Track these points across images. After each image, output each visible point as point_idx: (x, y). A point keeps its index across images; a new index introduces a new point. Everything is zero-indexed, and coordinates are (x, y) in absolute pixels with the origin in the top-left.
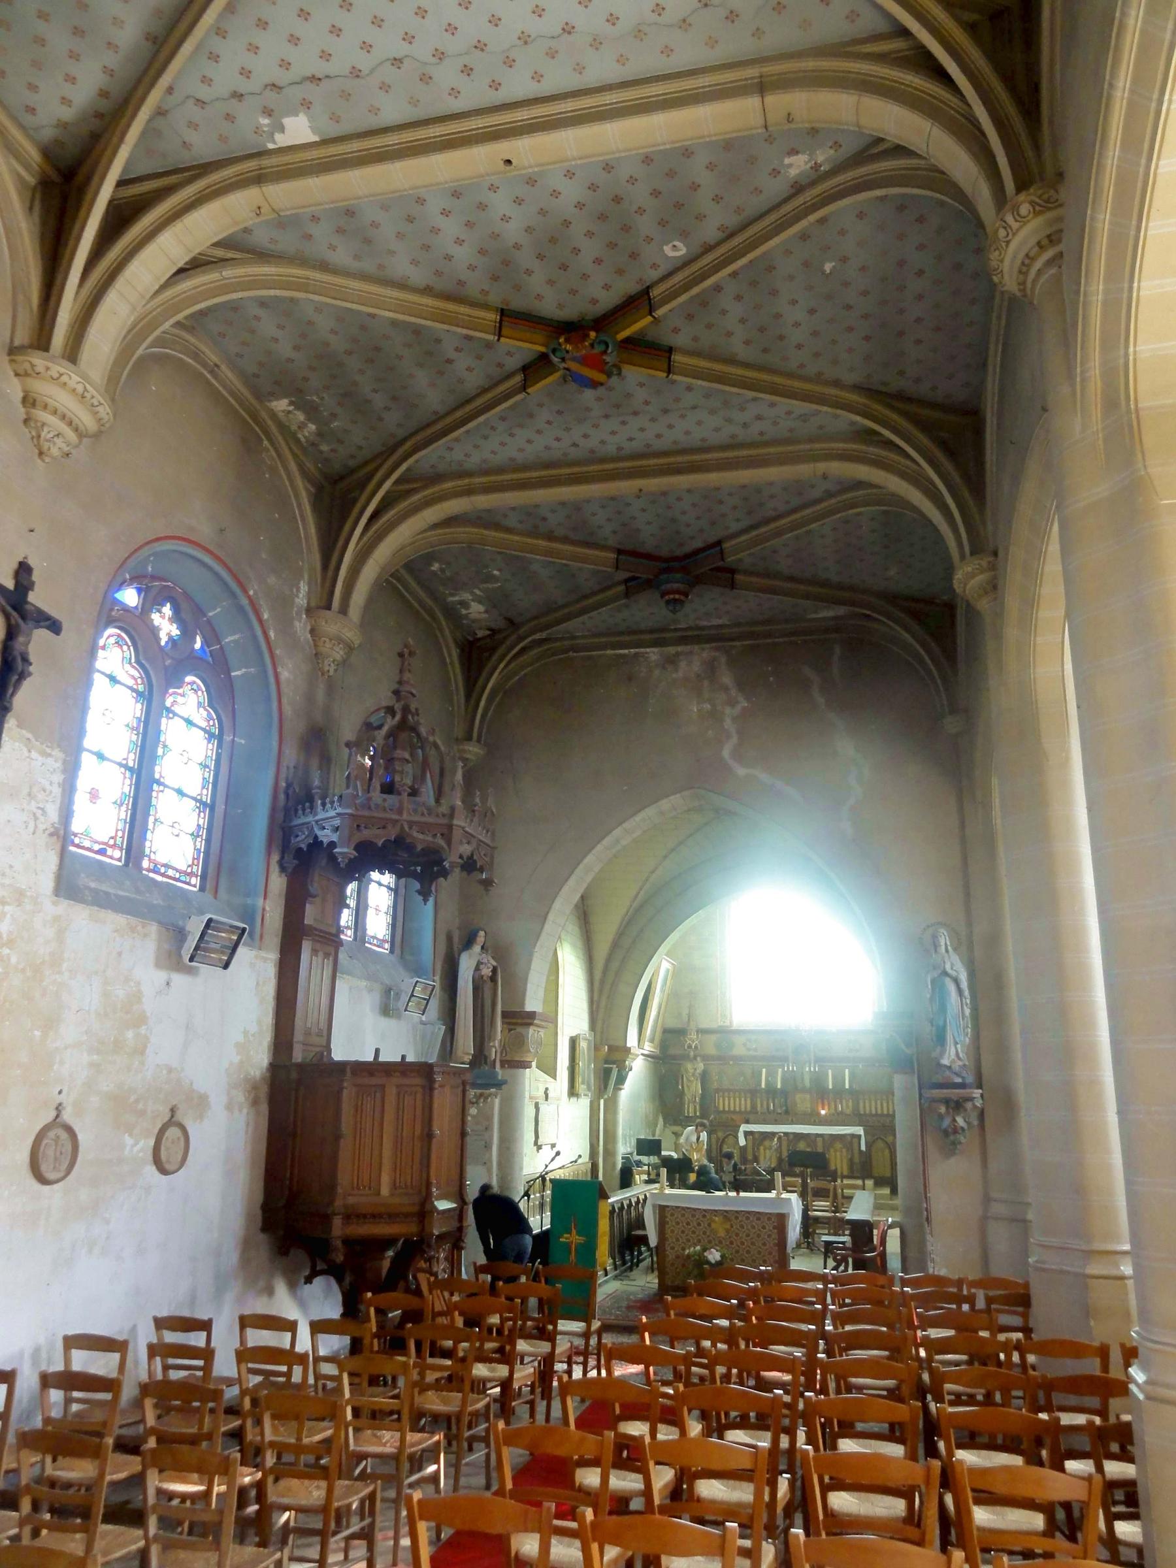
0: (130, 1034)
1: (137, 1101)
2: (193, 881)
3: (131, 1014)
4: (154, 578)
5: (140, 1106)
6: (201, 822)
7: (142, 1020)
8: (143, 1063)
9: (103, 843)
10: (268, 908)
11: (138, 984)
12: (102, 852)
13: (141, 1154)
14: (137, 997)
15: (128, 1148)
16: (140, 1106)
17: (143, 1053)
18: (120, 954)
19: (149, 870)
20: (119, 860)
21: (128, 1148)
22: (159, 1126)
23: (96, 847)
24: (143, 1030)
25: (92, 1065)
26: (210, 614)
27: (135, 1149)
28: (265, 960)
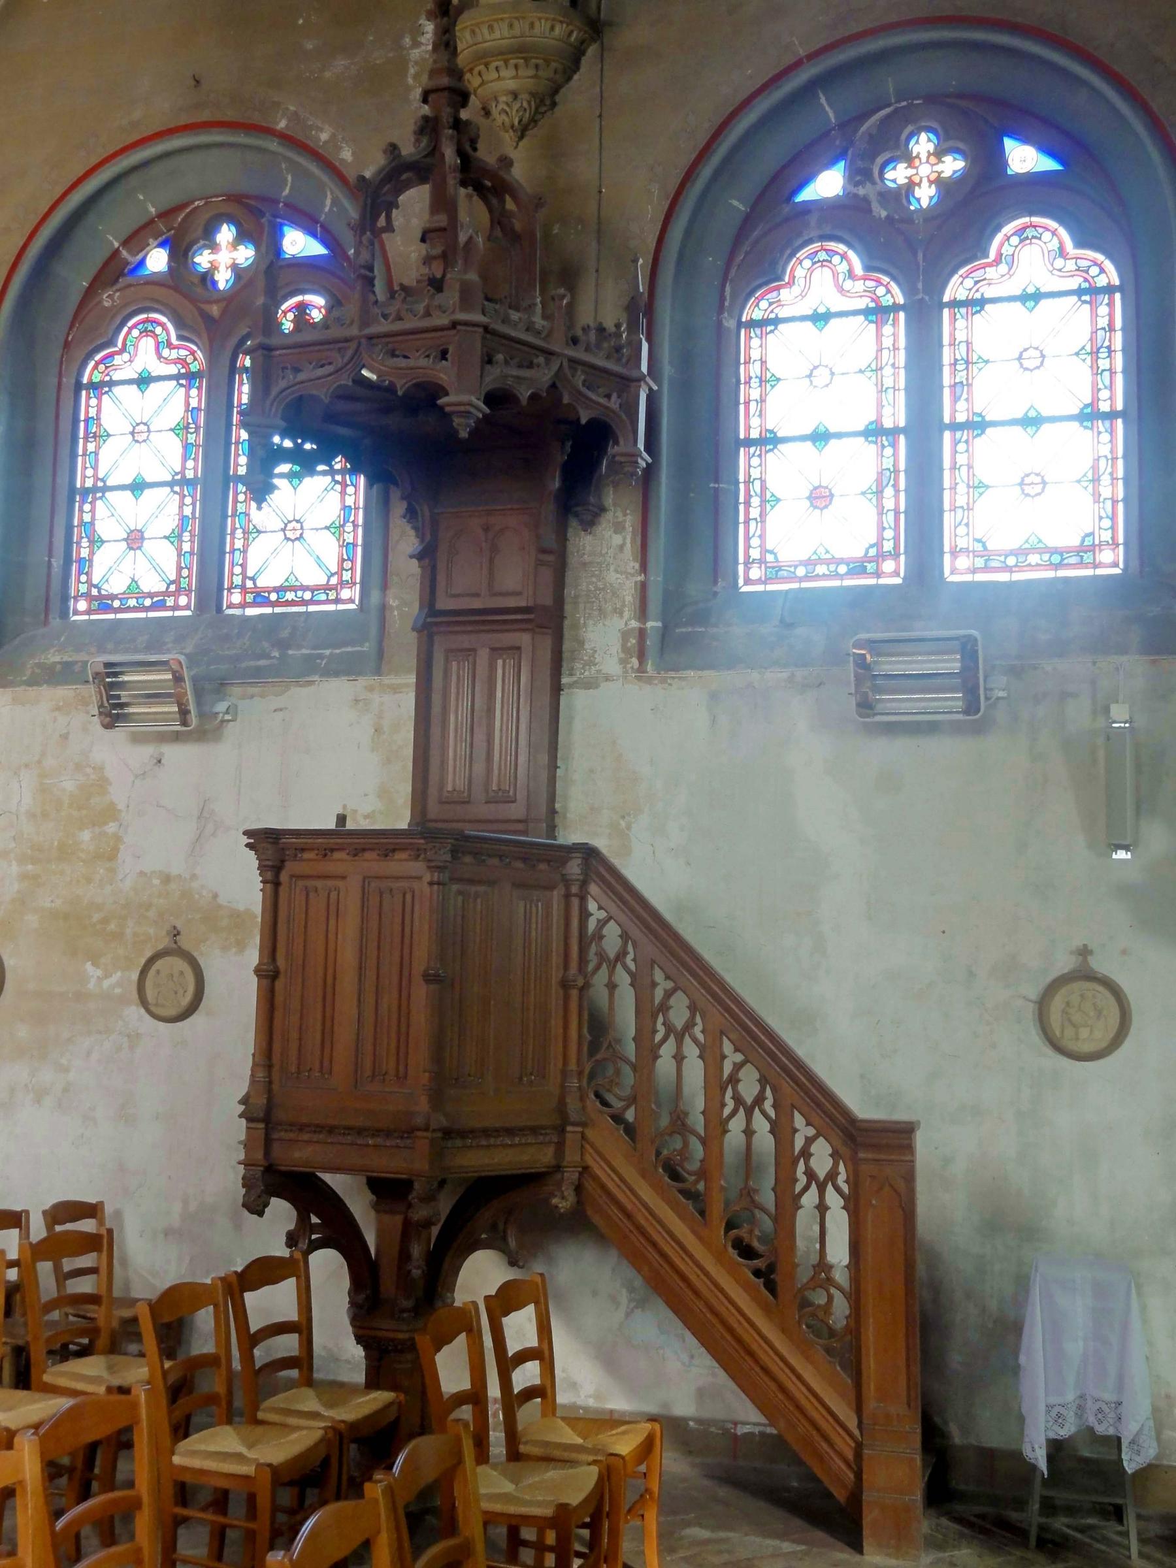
0: (86, 836)
1: (105, 921)
2: (345, 594)
3: (94, 807)
4: (165, 215)
5: (112, 926)
6: (350, 501)
7: (111, 813)
8: (112, 871)
9: (157, 594)
10: (393, 602)
11: (102, 769)
12: (159, 606)
13: (118, 991)
14: (102, 784)
15: (93, 981)
16: (112, 926)
17: (112, 856)
18: (65, 737)
19: (244, 605)
20: (187, 607)
21: (93, 981)
22: (149, 954)
23: (148, 602)
24: (111, 828)
25: (24, 877)
26: (287, 191)
27: (106, 984)
28: (395, 689)
